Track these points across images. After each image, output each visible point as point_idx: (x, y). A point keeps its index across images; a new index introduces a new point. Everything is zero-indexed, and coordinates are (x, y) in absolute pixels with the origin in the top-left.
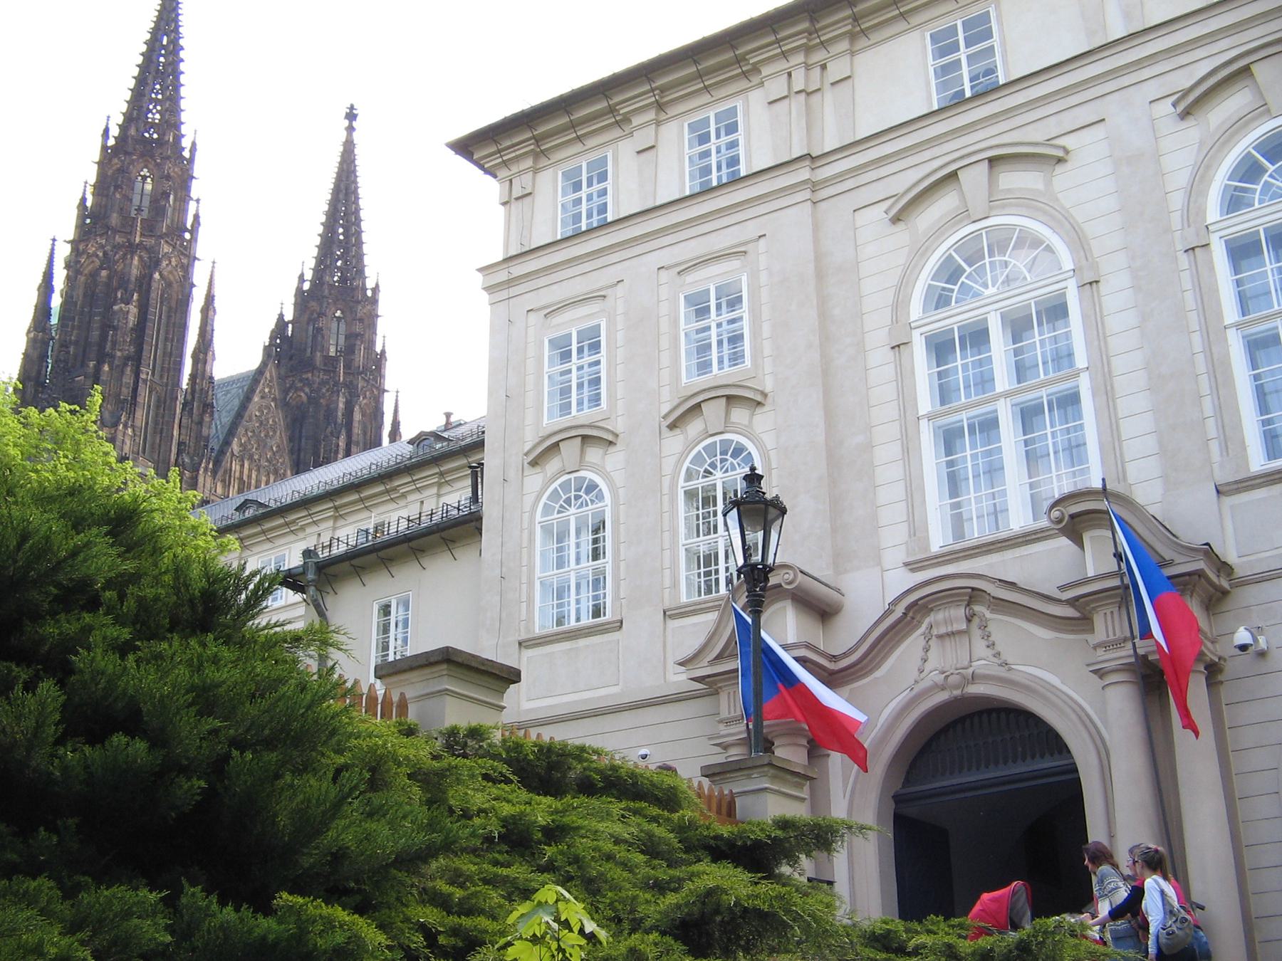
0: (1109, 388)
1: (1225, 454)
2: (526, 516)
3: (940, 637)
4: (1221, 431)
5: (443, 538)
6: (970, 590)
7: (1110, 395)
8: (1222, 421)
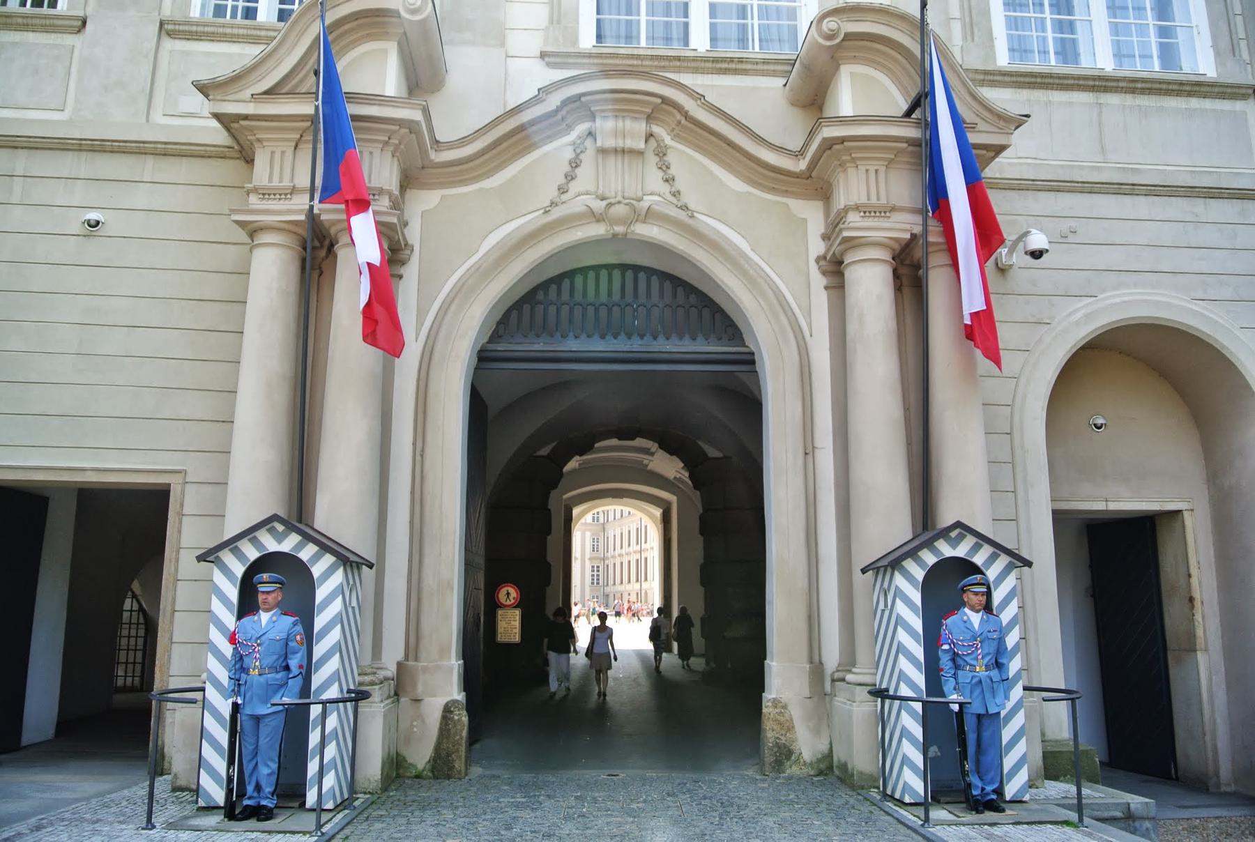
1: (969, 37)
3: (603, 151)
4: (967, 14)
6: (659, 101)
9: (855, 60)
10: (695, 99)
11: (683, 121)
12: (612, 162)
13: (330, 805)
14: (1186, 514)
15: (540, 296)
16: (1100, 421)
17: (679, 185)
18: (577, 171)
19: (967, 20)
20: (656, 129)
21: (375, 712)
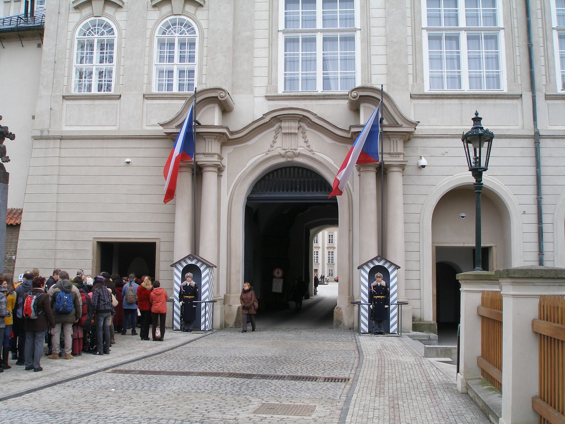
0: (369, 40)
2: (70, 33)
3: (285, 134)
4: (415, 72)
5: (19, 35)
6: (302, 116)
7: (369, 44)
8: (416, 68)
9: (365, 102)
10: (314, 115)
11: (310, 122)
12: (288, 138)
13: (207, 330)
14: (494, 248)
15: (267, 177)
16: (463, 216)
17: (310, 143)
18: (277, 139)
19: (415, 74)
20: (302, 124)
21: (218, 306)
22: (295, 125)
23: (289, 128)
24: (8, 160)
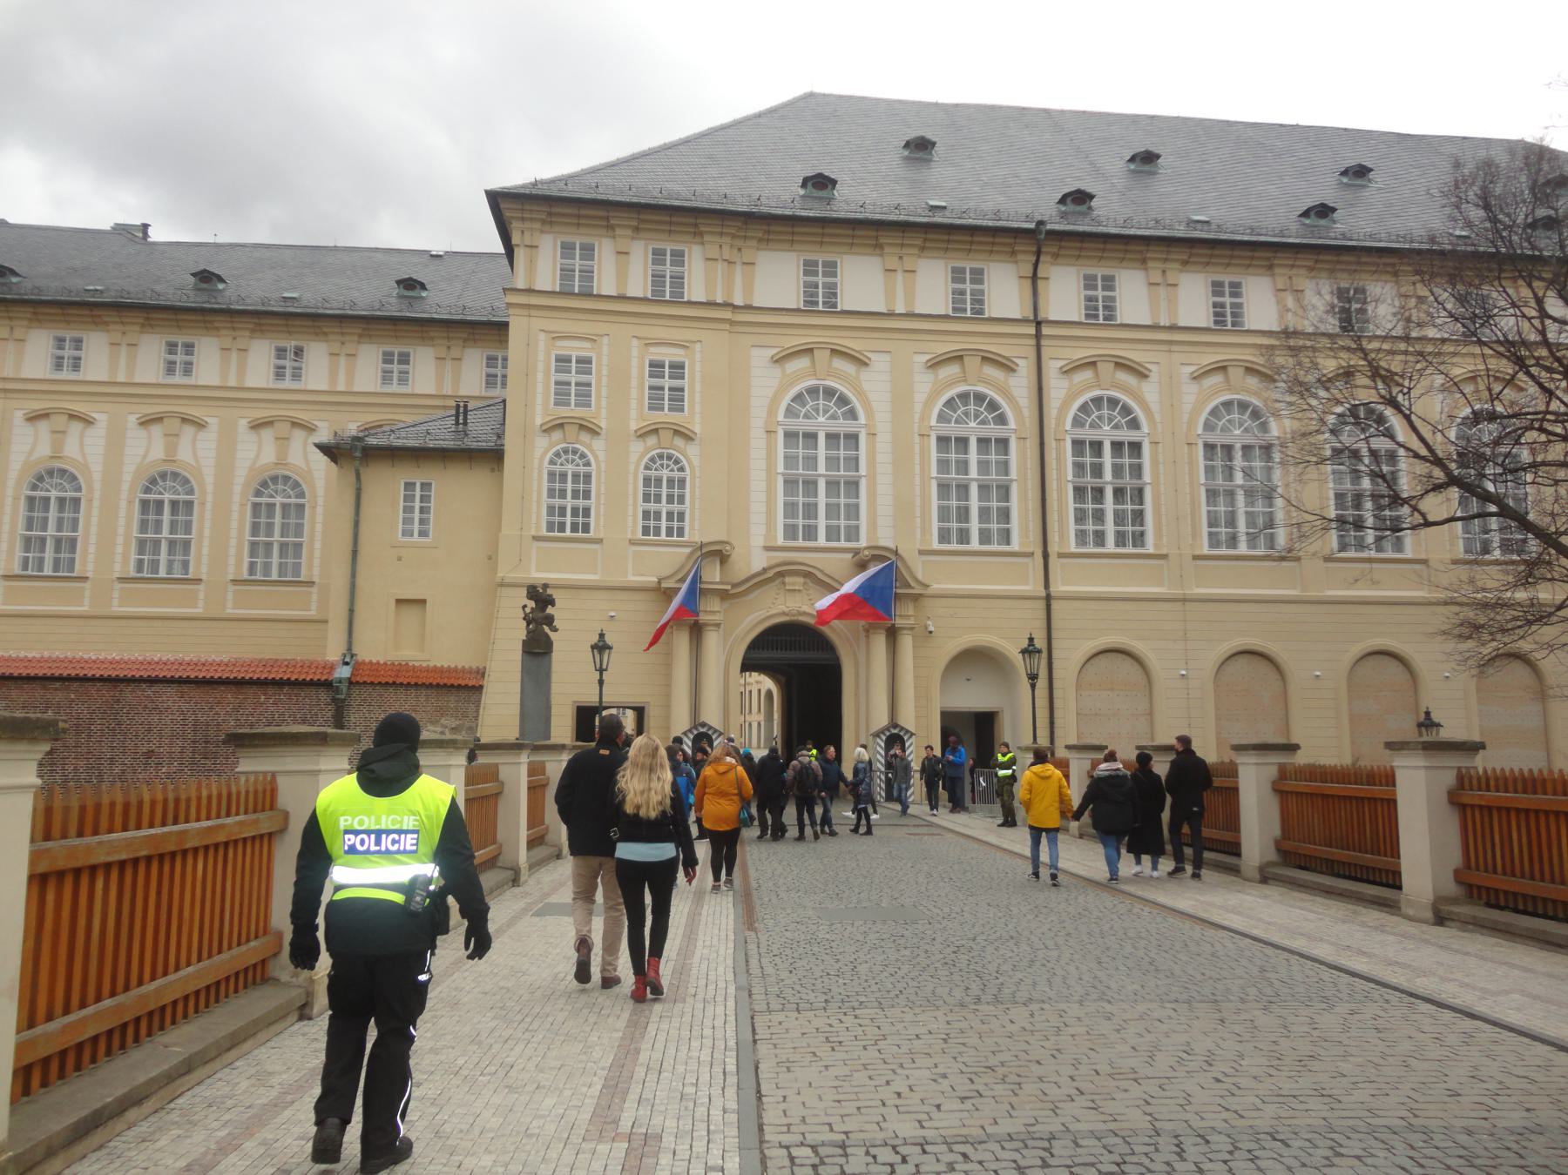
3: (789, 590)
22: (800, 580)
23: (793, 584)
24: (555, 630)
